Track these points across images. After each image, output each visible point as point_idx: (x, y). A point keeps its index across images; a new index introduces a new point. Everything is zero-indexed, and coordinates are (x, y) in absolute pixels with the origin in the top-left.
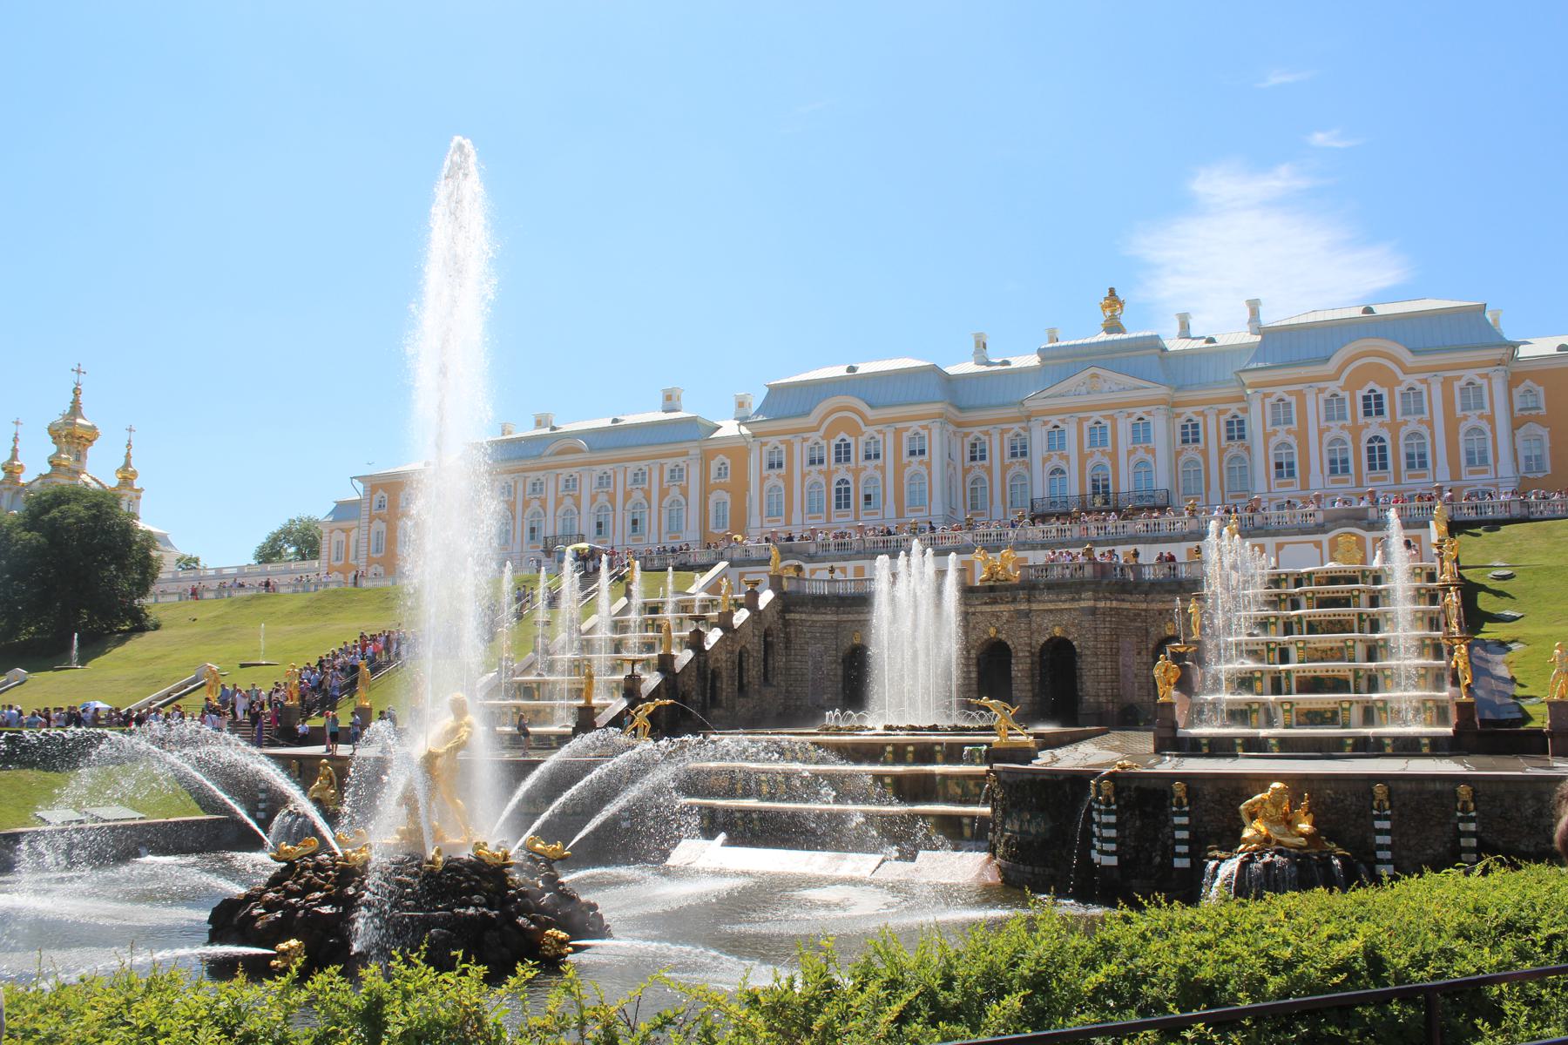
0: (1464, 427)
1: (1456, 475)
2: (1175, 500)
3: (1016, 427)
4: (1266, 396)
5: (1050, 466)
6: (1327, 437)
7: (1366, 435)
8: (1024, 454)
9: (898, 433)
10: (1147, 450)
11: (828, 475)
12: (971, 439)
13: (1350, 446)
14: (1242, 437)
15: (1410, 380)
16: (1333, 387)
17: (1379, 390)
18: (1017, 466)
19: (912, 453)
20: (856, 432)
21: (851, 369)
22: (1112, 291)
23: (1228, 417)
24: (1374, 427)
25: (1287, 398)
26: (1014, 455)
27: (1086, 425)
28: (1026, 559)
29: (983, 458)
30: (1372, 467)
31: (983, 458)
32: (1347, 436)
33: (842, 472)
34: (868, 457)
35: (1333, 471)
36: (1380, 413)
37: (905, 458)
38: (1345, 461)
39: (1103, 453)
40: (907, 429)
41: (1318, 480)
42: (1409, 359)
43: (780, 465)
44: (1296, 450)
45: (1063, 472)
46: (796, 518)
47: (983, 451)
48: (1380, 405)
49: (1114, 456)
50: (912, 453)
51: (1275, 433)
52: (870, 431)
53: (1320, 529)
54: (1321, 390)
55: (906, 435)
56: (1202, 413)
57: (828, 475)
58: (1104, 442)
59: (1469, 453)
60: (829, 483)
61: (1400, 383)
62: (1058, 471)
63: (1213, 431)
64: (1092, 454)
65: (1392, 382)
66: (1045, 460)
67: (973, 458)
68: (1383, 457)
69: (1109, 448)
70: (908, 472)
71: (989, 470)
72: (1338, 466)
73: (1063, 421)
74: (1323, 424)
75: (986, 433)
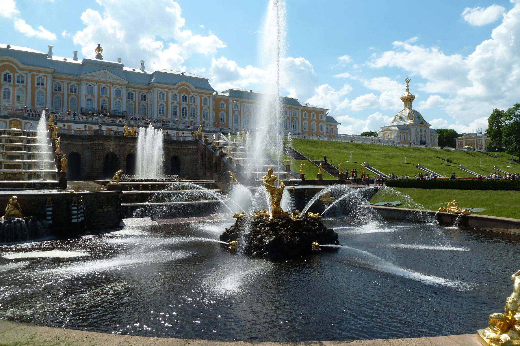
0: (204, 108)
1: (201, 120)
3: (74, 83)
4: (159, 90)
5: (87, 98)
6: (173, 105)
7: (182, 106)
8: (75, 92)
9: (33, 76)
10: (120, 99)
12: (56, 83)
13: (178, 108)
14: (145, 100)
15: (193, 94)
16: (175, 92)
17: (186, 95)
18: (73, 96)
19: (38, 84)
20: (14, 72)
21: (8, 47)
22: (99, 45)
23: (141, 93)
24: (184, 104)
25: (163, 92)
26: (71, 92)
27: (101, 87)
28: (111, 129)
29: (60, 90)
30: (183, 115)
31: (60, 90)
32: (178, 106)
34: (18, 82)
35: (174, 114)
36: (186, 101)
37: (36, 86)
38: (176, 112)
39: (106, 97)
40: (37, 75)
41: (170, 116)
42: (194, 89)
44: (165, 107)
45: (91, 100)
47: (60, 88)
48: (186, 99)
49: (109, 98)
50: (38, 84)
51: (160, 101)
52: (21, 72)
54: (173, 92)
55: (36, 77)
56: (135, 91)
58: (106, 93)
59: (204, 115)
61: (191, 94)
62: (90, 100)
63: (137, 97)
64: (102, 97)
65: (189, 94)
66: (86, 96)
67: (56, 90)
68: (186, 113)
69: (108, 96)
70: (37, 90)
71: (63, 95)
72: (175, 113)
73: (93, 84)
74: (172, 101)
75: (63, 82)
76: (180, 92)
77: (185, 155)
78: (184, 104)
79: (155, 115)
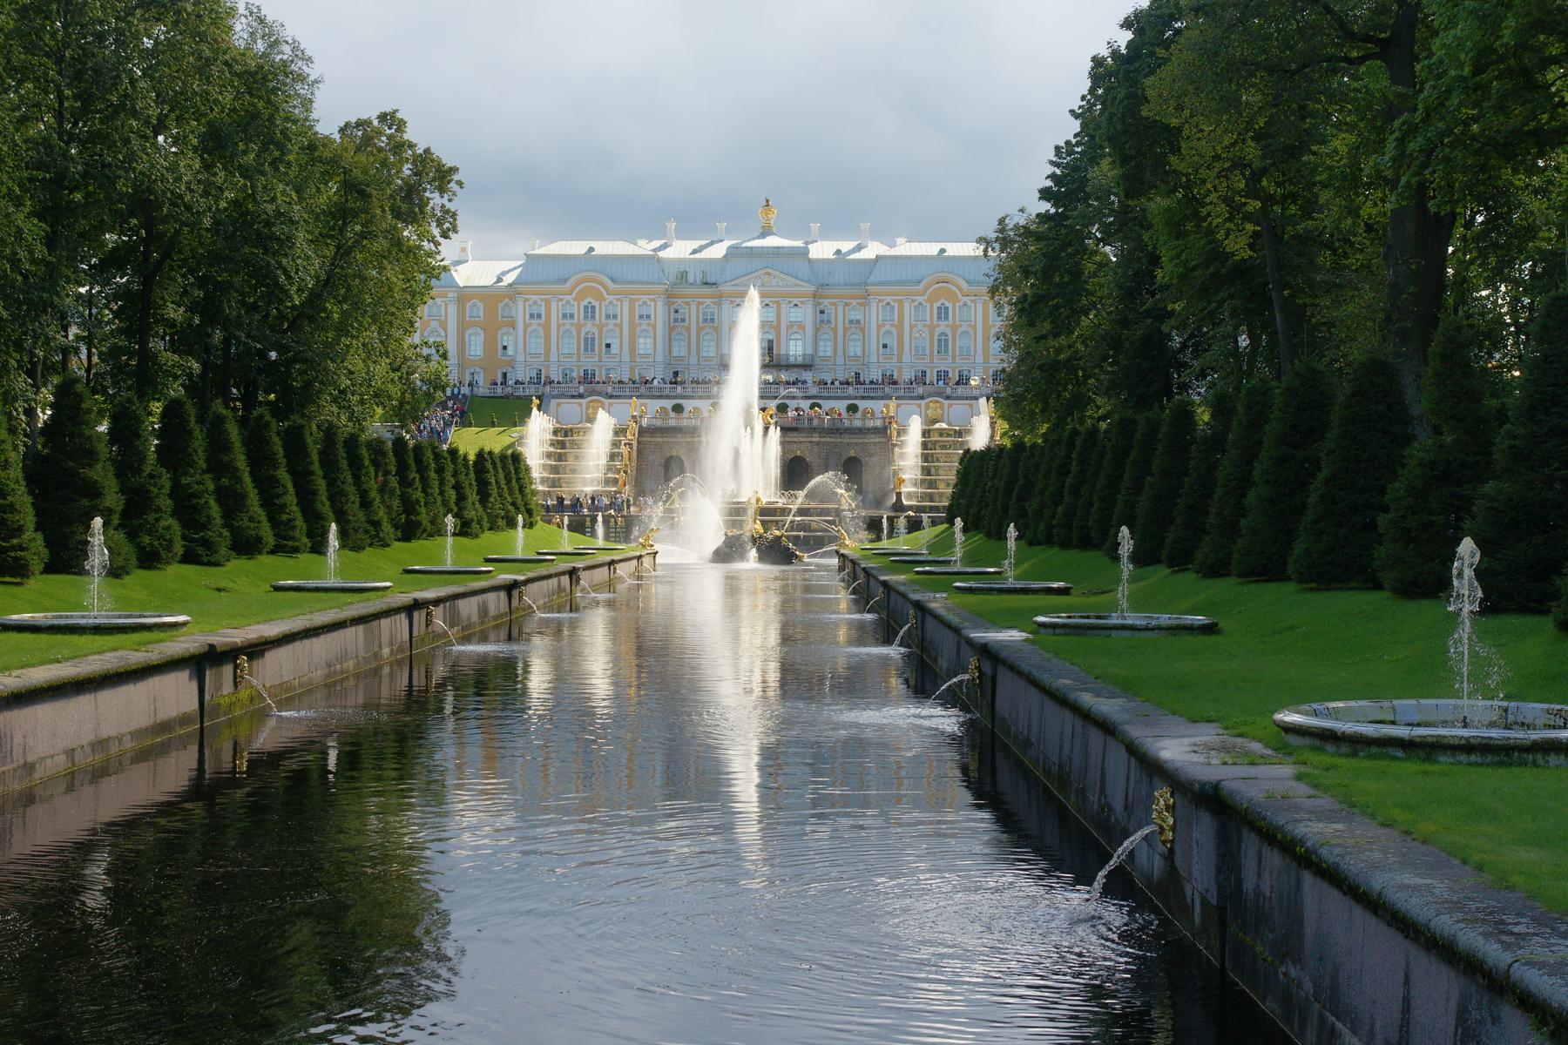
2: (817, 361)
7: (938, 331)
9: (632, 302)
11: (579, 327)
16: (920, 299)
20: (600, 298)
24: (942, 327)
33: (589, 327)
34: (608, 316)
36: (946, 318)
42: (965, 285)
43: (539, 316)
46: (553, 358)
48: (947, 313)
52: (611, 298)
53: (922, 398)
56: (834, 304)
57: (579, 327)
60: (579, 333)
65: (954, 299)
71: (688, 330)
76: (931, 300)
77: (871, 455)
78: (942, 327)
79: (874, 359)
